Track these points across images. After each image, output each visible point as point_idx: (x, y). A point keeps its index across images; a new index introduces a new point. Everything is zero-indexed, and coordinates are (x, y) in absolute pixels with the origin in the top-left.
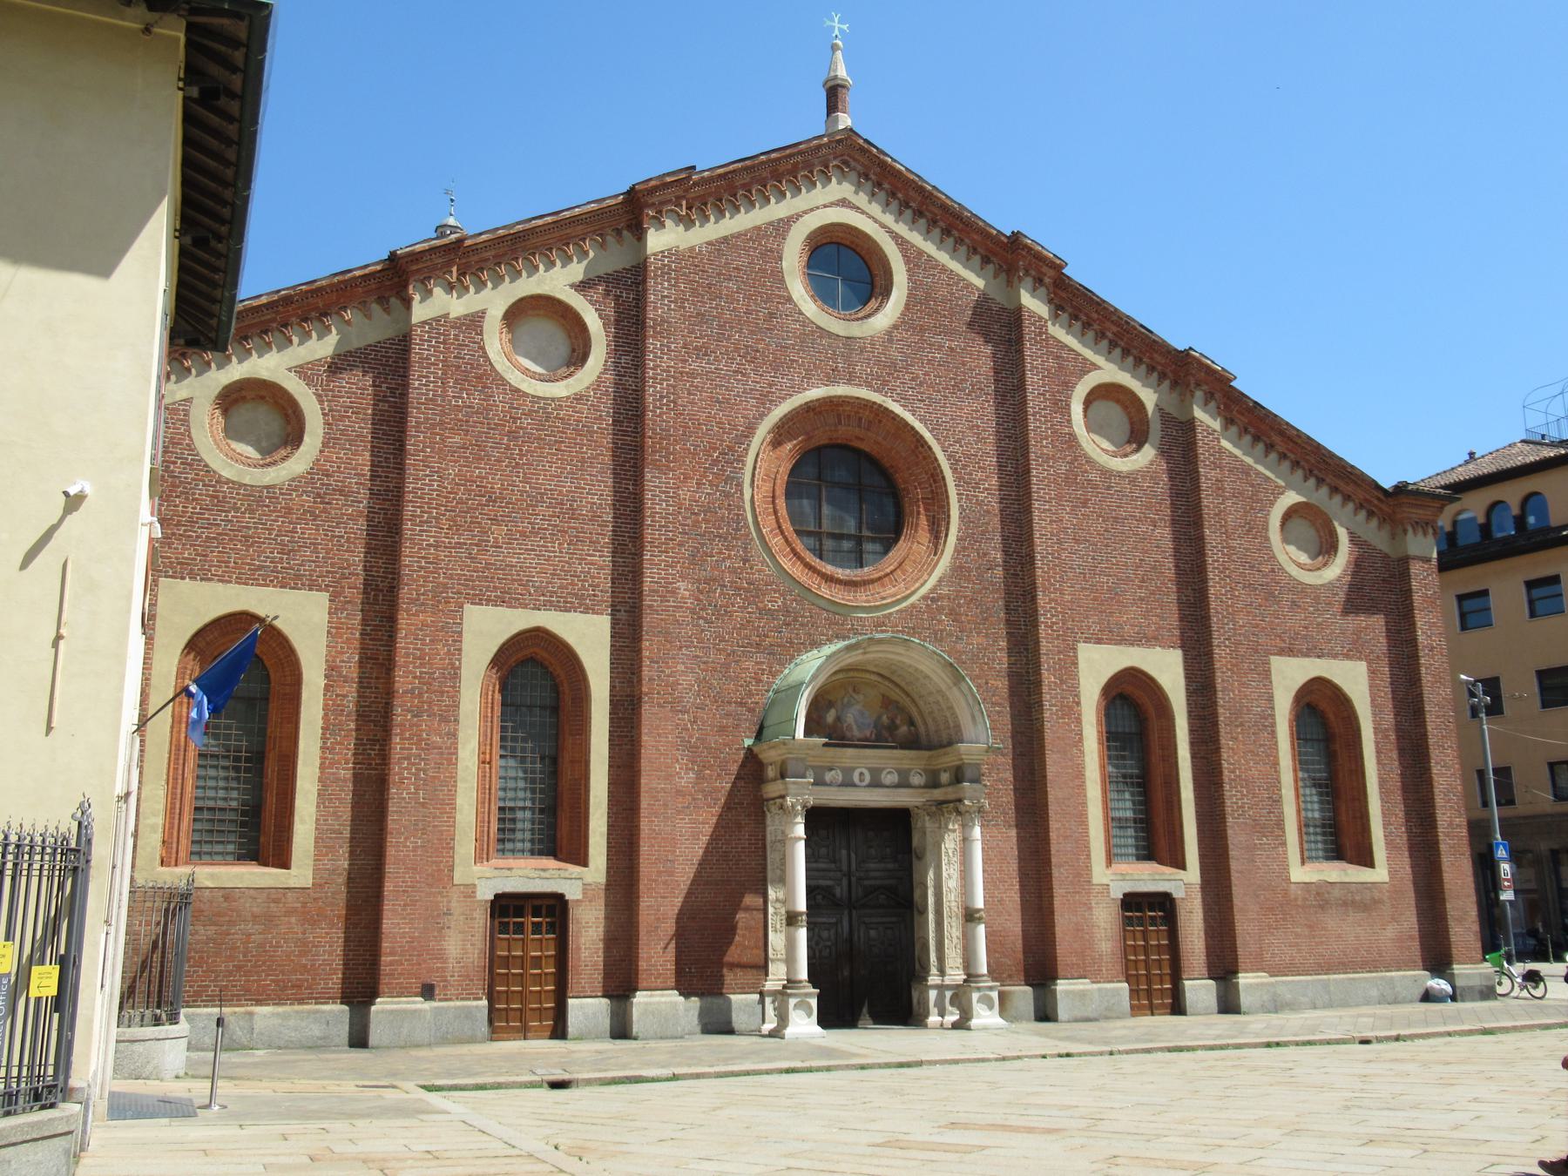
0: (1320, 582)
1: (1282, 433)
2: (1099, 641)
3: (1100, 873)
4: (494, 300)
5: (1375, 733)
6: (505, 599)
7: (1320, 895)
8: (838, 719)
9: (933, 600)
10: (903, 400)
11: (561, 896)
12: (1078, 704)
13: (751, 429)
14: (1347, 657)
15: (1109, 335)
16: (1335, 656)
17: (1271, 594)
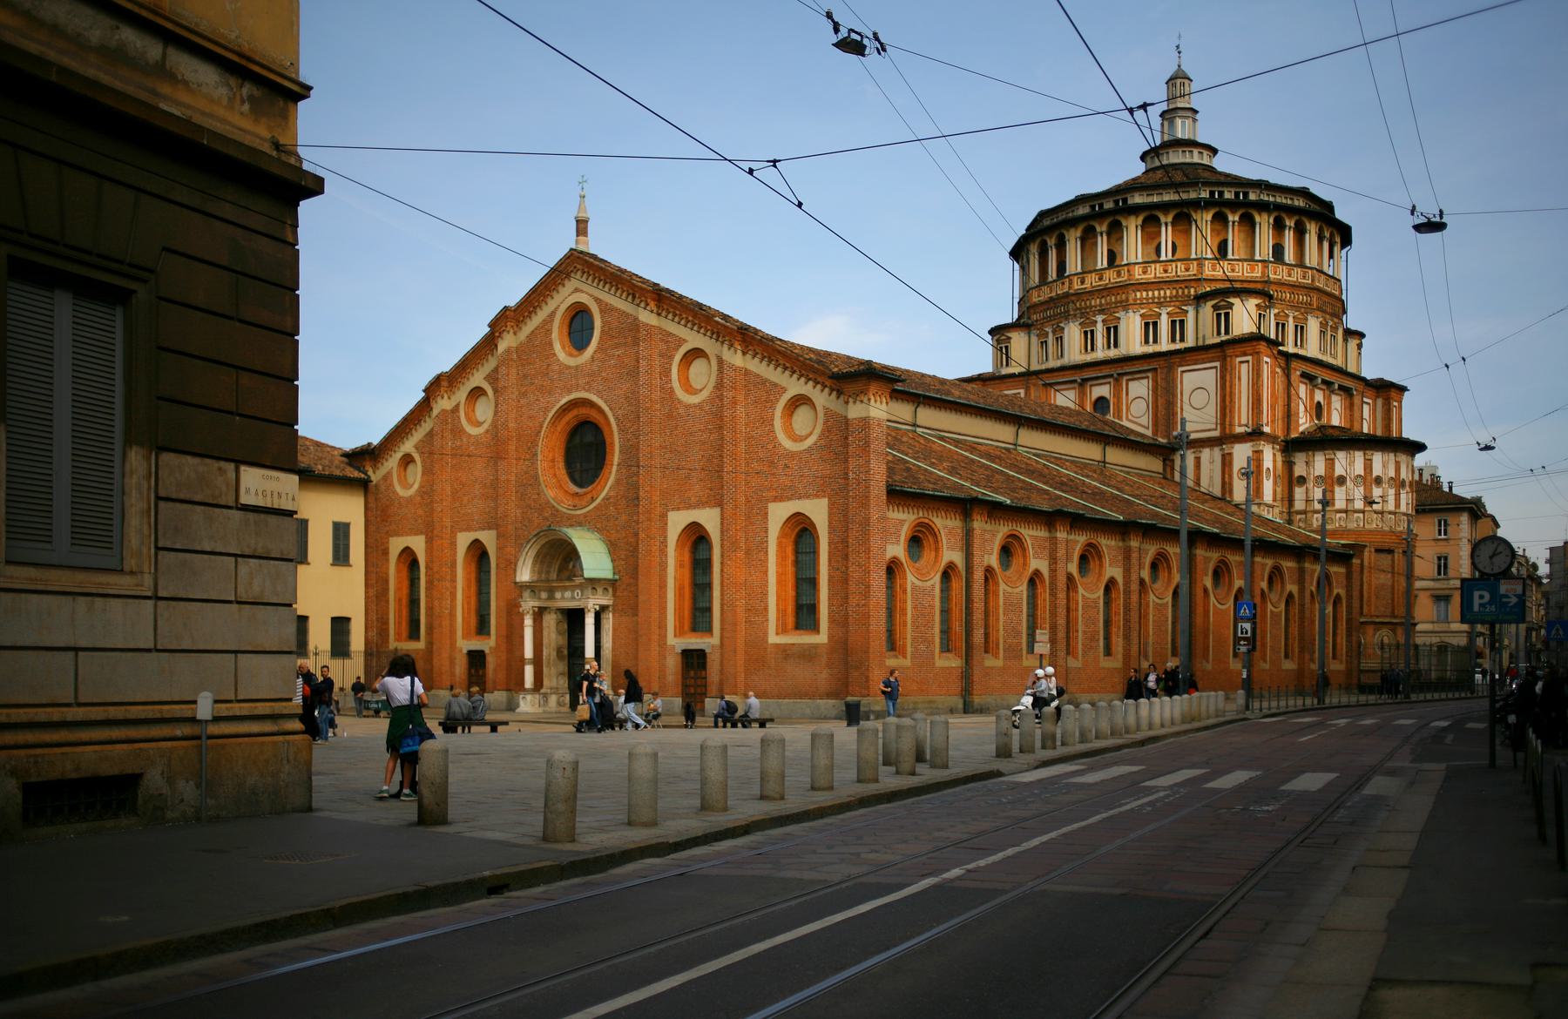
0: (802, 448)
1: (779, 352)
2: (678, 509)
3: (671, 640)
4: (461, 395)
5: (829, 546)
6: (468, 529)
7: (785, 652)
8: (574, 567)
9: (607, 499)
10: (599, 393)
11: (483, 651)
12: (666, 546)
13: (542, 427)
14: (817, 496)
15: (690, 318)
16: (808, 497)
17: (772, 462)
